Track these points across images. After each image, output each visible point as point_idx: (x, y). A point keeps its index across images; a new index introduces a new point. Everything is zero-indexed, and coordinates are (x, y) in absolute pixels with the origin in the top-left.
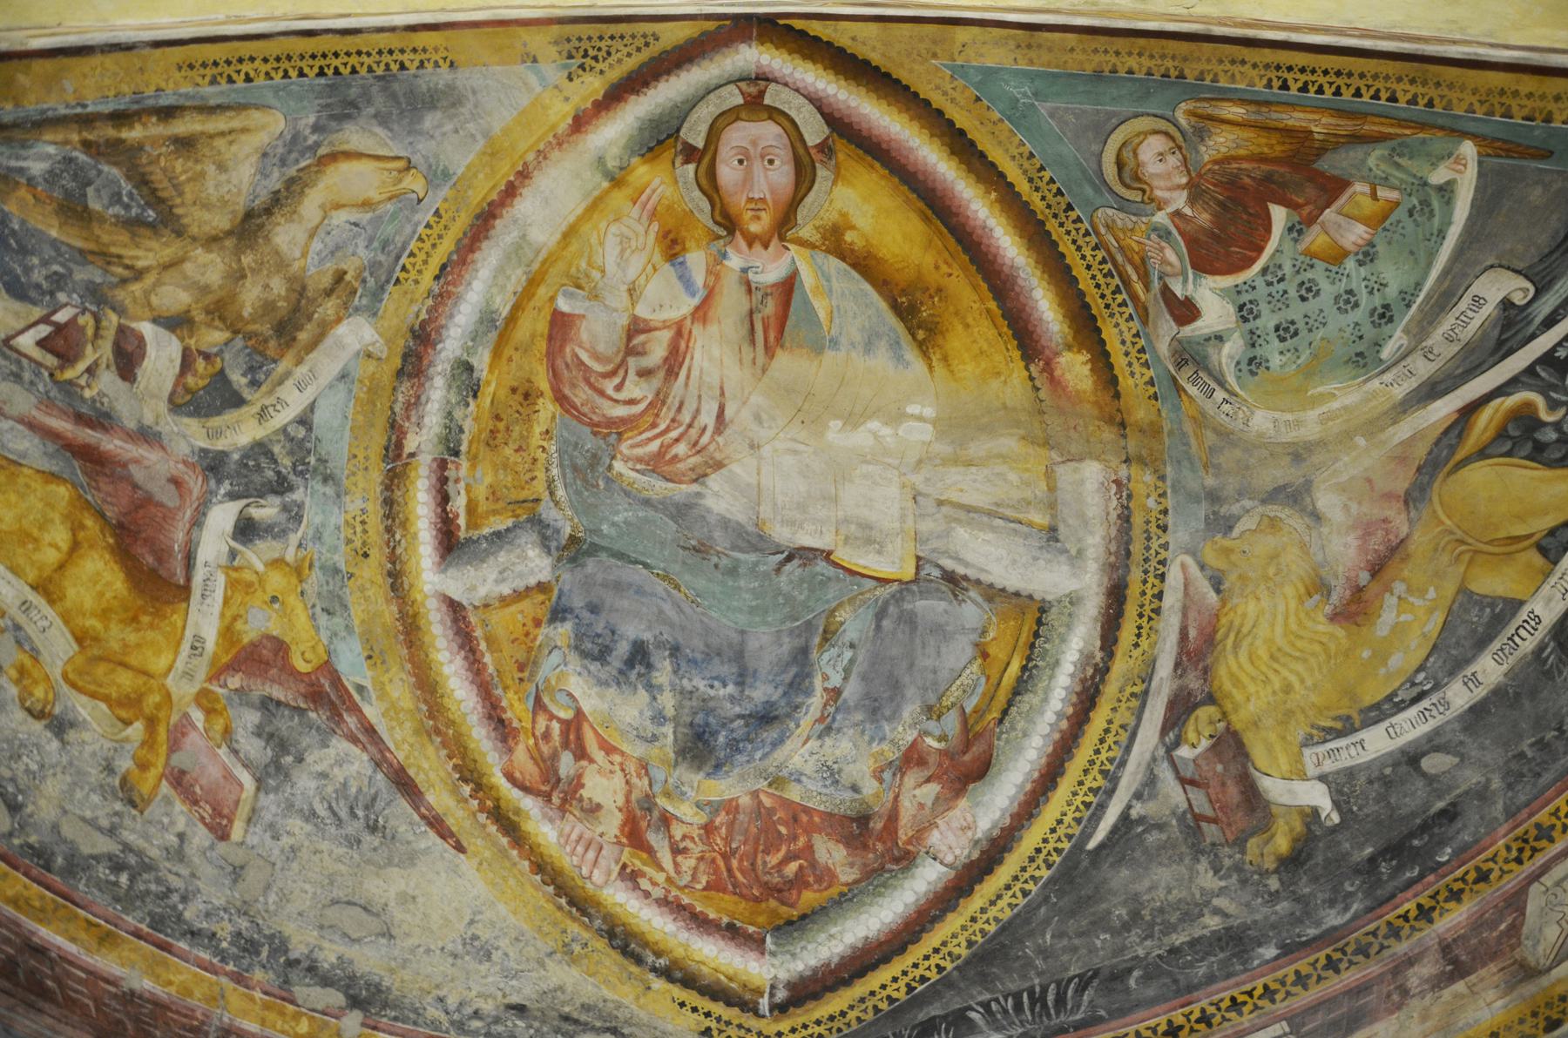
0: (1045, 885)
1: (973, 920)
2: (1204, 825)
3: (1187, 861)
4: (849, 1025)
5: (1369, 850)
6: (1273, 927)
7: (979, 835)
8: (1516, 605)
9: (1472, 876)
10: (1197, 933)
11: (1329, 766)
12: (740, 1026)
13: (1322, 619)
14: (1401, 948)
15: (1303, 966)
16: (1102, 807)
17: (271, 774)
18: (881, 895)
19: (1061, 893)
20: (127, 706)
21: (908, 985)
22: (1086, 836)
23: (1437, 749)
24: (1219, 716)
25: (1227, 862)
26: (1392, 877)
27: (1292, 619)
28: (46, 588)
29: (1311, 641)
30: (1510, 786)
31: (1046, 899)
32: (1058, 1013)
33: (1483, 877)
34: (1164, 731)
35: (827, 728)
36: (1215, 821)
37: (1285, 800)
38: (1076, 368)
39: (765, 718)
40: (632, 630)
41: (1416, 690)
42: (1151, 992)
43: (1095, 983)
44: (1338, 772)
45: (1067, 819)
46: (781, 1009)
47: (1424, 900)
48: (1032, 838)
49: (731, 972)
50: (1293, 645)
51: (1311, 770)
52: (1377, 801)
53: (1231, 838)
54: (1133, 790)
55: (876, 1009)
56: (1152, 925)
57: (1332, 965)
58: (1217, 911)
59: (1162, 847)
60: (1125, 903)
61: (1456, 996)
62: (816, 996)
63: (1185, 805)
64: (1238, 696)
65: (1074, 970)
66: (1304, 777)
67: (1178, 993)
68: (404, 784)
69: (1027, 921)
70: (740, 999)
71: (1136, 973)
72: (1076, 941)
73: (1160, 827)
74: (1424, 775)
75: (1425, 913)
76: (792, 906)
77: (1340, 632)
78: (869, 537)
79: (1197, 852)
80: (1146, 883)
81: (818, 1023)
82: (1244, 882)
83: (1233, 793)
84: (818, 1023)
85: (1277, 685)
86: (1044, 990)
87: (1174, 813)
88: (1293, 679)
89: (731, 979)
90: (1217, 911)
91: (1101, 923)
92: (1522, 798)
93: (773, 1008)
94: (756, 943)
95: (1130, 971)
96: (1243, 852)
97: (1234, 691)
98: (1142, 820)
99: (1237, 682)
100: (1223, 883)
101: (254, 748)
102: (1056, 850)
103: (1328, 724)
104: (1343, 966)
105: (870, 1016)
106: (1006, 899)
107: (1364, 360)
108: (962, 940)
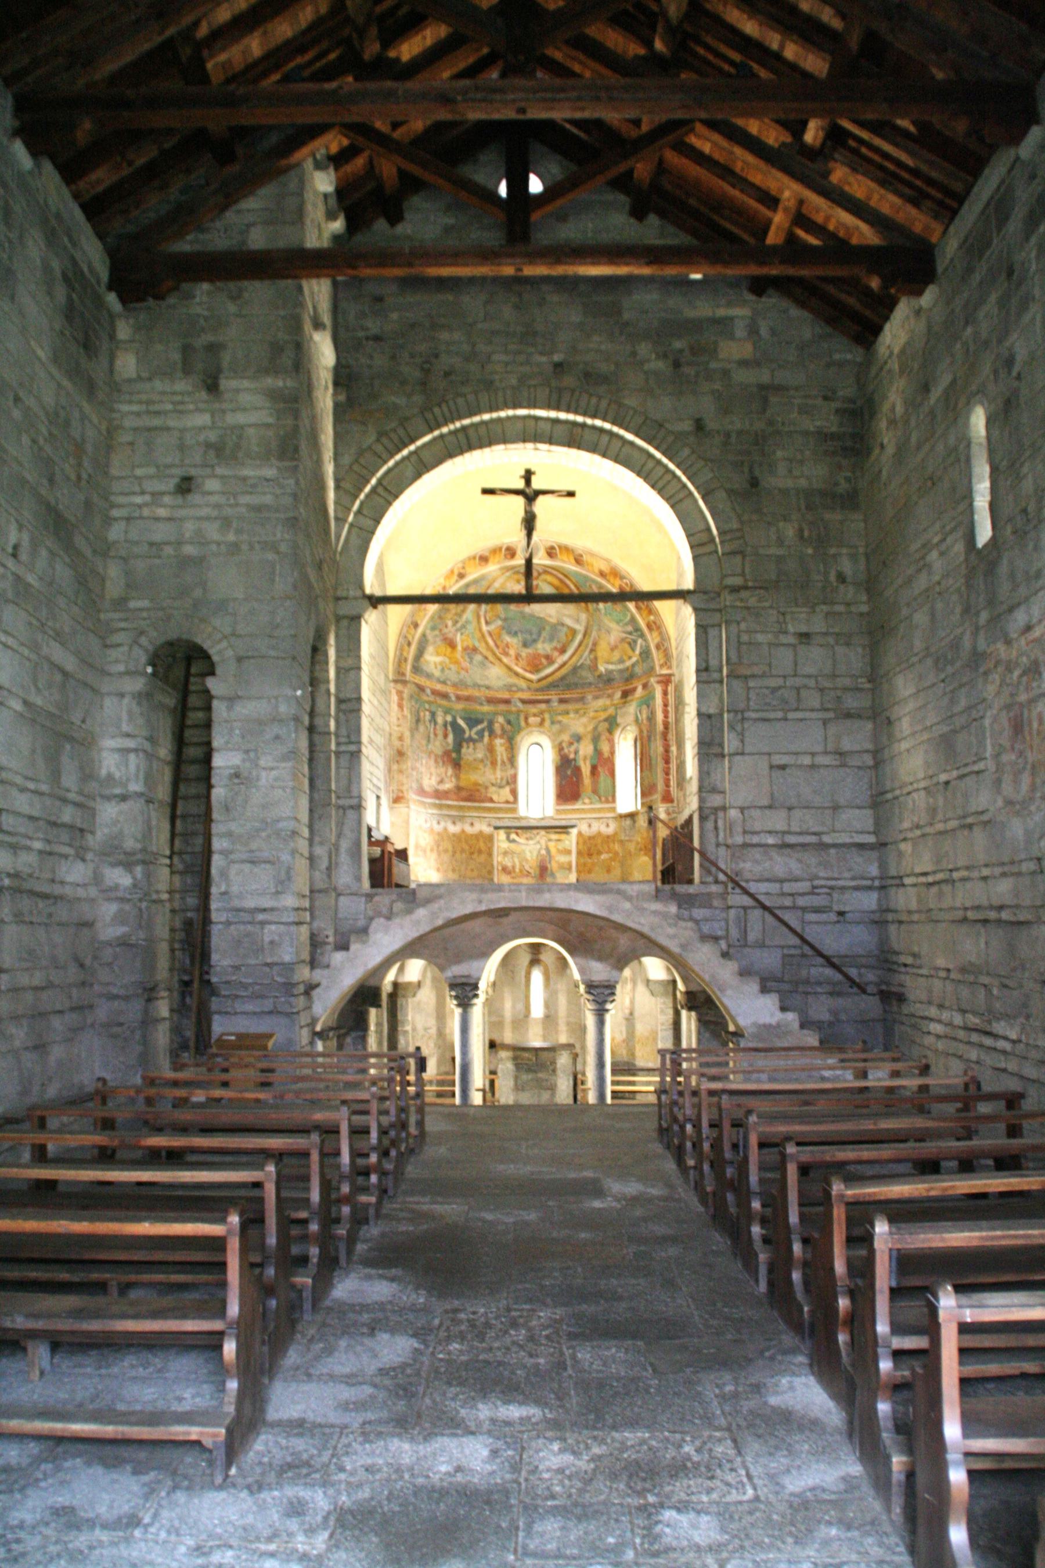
17: (471, 662)
39: (535, 641)
40: (515, 629)
68: (486, 658)
70: (531, 681)
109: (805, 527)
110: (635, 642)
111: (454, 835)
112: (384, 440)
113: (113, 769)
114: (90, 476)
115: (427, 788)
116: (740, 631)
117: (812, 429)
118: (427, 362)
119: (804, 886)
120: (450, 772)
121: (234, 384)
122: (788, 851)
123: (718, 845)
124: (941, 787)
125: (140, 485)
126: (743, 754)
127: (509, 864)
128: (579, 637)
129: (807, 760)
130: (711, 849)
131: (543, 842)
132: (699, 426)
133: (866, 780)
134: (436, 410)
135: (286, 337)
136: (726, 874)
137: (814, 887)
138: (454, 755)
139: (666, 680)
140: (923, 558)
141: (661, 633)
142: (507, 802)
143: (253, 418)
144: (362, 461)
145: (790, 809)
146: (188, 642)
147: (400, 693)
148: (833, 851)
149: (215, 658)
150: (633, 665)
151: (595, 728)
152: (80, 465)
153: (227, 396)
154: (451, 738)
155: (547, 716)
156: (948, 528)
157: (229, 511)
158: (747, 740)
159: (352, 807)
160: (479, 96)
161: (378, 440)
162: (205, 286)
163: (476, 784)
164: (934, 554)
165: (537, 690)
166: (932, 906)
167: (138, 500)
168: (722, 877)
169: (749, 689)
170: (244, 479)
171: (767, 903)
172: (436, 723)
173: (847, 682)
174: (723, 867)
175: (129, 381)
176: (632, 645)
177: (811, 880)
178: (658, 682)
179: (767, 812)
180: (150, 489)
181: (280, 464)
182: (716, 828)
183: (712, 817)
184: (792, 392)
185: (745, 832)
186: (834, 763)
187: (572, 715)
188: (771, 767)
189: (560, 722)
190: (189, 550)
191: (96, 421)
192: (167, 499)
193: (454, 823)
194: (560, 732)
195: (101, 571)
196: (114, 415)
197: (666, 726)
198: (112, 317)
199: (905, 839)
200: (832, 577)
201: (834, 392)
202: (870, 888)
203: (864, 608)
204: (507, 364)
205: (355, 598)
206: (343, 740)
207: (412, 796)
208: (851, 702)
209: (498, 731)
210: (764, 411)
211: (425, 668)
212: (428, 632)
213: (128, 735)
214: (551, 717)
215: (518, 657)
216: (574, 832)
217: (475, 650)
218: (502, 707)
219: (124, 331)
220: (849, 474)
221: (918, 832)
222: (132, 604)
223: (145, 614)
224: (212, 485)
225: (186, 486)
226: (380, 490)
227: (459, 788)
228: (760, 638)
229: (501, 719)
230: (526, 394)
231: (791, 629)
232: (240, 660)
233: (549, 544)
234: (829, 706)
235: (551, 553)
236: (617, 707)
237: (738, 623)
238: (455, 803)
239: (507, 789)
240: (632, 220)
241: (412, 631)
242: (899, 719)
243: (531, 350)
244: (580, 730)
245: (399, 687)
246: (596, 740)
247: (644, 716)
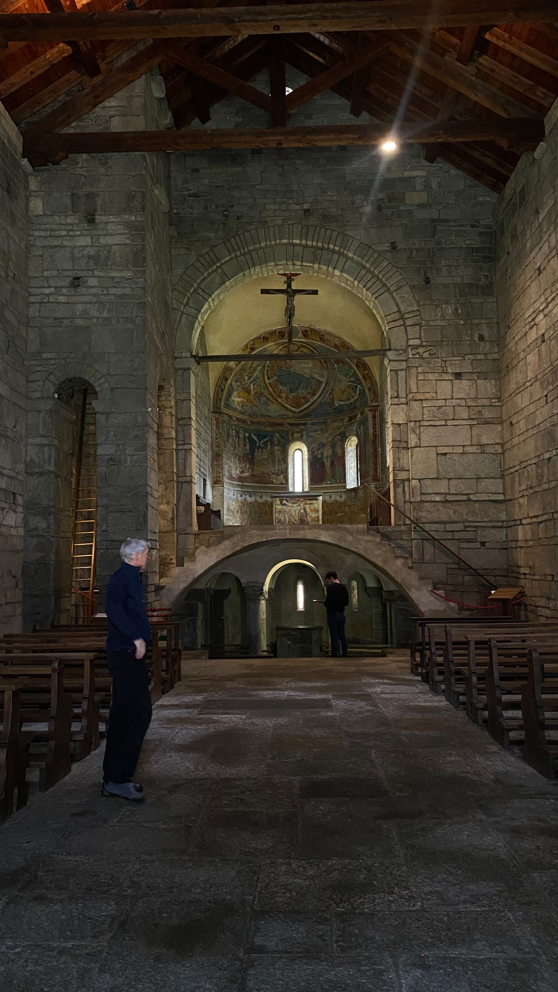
20: (250, 402)
28: (244, 398)
35: (302, 389)
38: (325, 365)
40: (285, 382)
68: (269, 399)
70: (295, 412)
78: (306, 373)
101: (258, 400)
107: (346, 376)
109: (458, 306)
110: (356, 387)
111: (251, 503)
112: (202, 260)
113: (34, 456)
114: (14, 275)
115: (234, 476)
116: (417, 373)
117: (464, 246)
118: (227, 211)
119: (460, 526)
120: (248, 466)
121: (105, 218)
122: (448, 505)
123: (405, 502)
124: (546, 461)
125: (48, 282)
126: (420, 447)
127: (283, 518)
128: (323, 385)
129: (460, 450)
130: (401, 504)
131: (302, 505)
132: (394, 247)
133: (497, 462)
134: (232, 240)
135: (135, 189)
136: (410, 519)
137: (465, 527)
138: (250, 456)
139: (375, 409)
140: (534, 320)
141: (371, 381)
142: (282, 484)
143: (118, 239)
144: (188, 273)
145: (449, 479)
146: (80, 378)
147: (217, 419)
148: (477, 505)
149: (97, 389)
150: (355, 402)
151: (333, 439)
152: (7, 266)
153: (100, 226)
154: (248, 447)
155: (304, 433)
156: (550, 299)
157: (104, 298)
158: (423, 437)
159: (186, 482)
160: (249, 18)
161: (197, 260)
162: (84, 156)
163: (263, 473)
164: (541, 316)
165: (299, 418)
166: (541, 536)
167: (47, 291)
168: (408, 522)
169: (423, 407)
170: (113, 278)
171: (436, 537)
172: (239, 438)
173: (485, 402)
174: (408, 515)
175: (38, 216)
176: (354, 389)
177: (463, 522)
178: (370, 410)
179: (435, 481)
180: (54, 285)
181: (133, 269)
182: (404, 492)
183: (402, 486)
184: (451, 223)
185: (422, 494)
186: (477, 451)
188: (438, 454)
189: (312, 436)
190: (80, 322)
191: (18, 241)
192: (64, 291)
193: (250, 496)
195: (24, 334)
196: (30, 238)
197: (375, 435)
198: (26, 175)
199: (523, 496)
200: (476, 338)
201: (479, 222)
202: (501, 527)
203: (496, 356)
204: (275, 211)
205: (186, 358)
206: (180, 442)
207: (226, 480)
208: (487, 414)
209: (276, 443)
210: (434, 236)
211: (232, 405)
212: (233, 383)
213: (43, 436)
214: (307, 434)
215: (287, 398)
216: (321, 498)
217: (262, 394)
218: (278, 428)
219: (33, 185)
220: (486, 274)
221: (531, 491)
222: (44, 356)
223: (53, 362)
224: (93, 282)
225: (76, 282)
226: (200, 291)
227: (253, 476)
228: (431, 377)
229: (277, 435)
230: (287, 230)
231: (450, 370)
232: (112, 389)
233: (304, 329)
234: (473, 417)
235: (305, 334)
237: (417, 367)
238: (251, 484)
239: (282, 476)
240: (352, 116)
241: (224, 382)
242: (518, 422)
243: (291, 202)
244: (324, 441)
245: (216, 415)
246: (333, 446)
247: (362, 431)
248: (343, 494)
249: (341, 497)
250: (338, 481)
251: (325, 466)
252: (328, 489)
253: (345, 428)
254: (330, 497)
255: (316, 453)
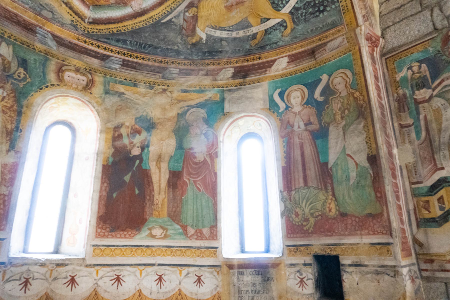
0: (150, 25)
1: (134, 24)
2: (183, 29)
3: (177, 34)
4: (103, 32)
5: (206, 50)
6: (185, 53)
7: (142, 7)
8: (252, 26)
9: (217, 63)
10: (173, 48)
11: (209, 33)
12: (80, 23)
13: (223, 5)
14: (201, 67)
15: (186, 62)
16: (167, 15)
18: (118, 9)
19: (153, 28)
21: (117, 30)
22: (162, 19)
23: (226, 41)
24: (196, 11)
25: (184, 39)
26: (207, 56)
27: (219, 2)
29: (219, 9)
30: (231, 53)
31: (149, 27)
32: (143, 49)
33: (219, 64)
34: (186, 7)
36: (186, 30)
37: (199, 34)
41: (229, 29)
42: (160, 54)
43: (152, 47)
44: (209, 35)
45: (160, 14)
46: (90, 23)
47: (209, 62)
48: (152, 14)
49: (81, 10)
50: (216, 7)
51: (206, 32)
52: (212, 43)
53: (187, 34)
54: (175, 15)
55: (109, 32)
56: (166, 42)
57: (190, 64)
58: (178, 46)
59: (174, 29)
60: (163, 36)
61: (205, 78)
62: (98, 24)
63: (182, 24)
64: (202, 11)
65: (149, 43)
66: (204, 32)
67: (165, 56)
69: (144, 30)
71: (159, 49)
72: (152, 38)
73: (176, 25)
74: (221, 44)
75: (208, 64)
76: (98, 2)
77: (225, 11)
79: (180, 34)
80: (168, 34)
81: (97, 29)
82: (185, 43)
83: (191, 27)
84: (97, 29)
85: (209, 12)
86: (142, 44)
87: (179, 24)
88: (212, 13)
89: (80, 12)
90: (178, 46)
91: (157, 37)
92: (231, 56)
93: (88, 22)
94: (88, 7)
95: (159, 48)
96: (187, 39)
97: (202, 9)
98: (173, 22)
99: (203, 7)
100: (181, 42)
102: (155, 19)
103: (213, 25)
104: (192, 65)
105: (108, 33)
106: (142, 23)
108: (131, 26)
155: (99, 79)
187: (142, 89)
189: (120, 94)
194: (119, 110)
214: (106, 84)
236: (223, 89)
248: (206, 275)
249: (199, 280)
250: (191, 231)
251: (150, 182)
252: (153, 254)
253: (223, 91)
254: (160, 279)
255: (126, 141)
